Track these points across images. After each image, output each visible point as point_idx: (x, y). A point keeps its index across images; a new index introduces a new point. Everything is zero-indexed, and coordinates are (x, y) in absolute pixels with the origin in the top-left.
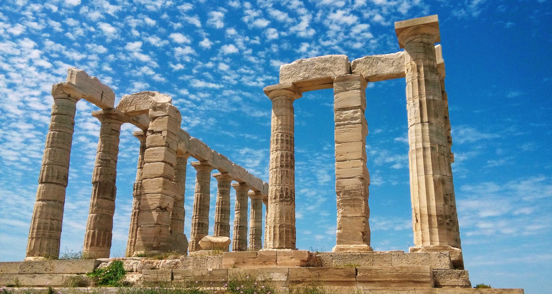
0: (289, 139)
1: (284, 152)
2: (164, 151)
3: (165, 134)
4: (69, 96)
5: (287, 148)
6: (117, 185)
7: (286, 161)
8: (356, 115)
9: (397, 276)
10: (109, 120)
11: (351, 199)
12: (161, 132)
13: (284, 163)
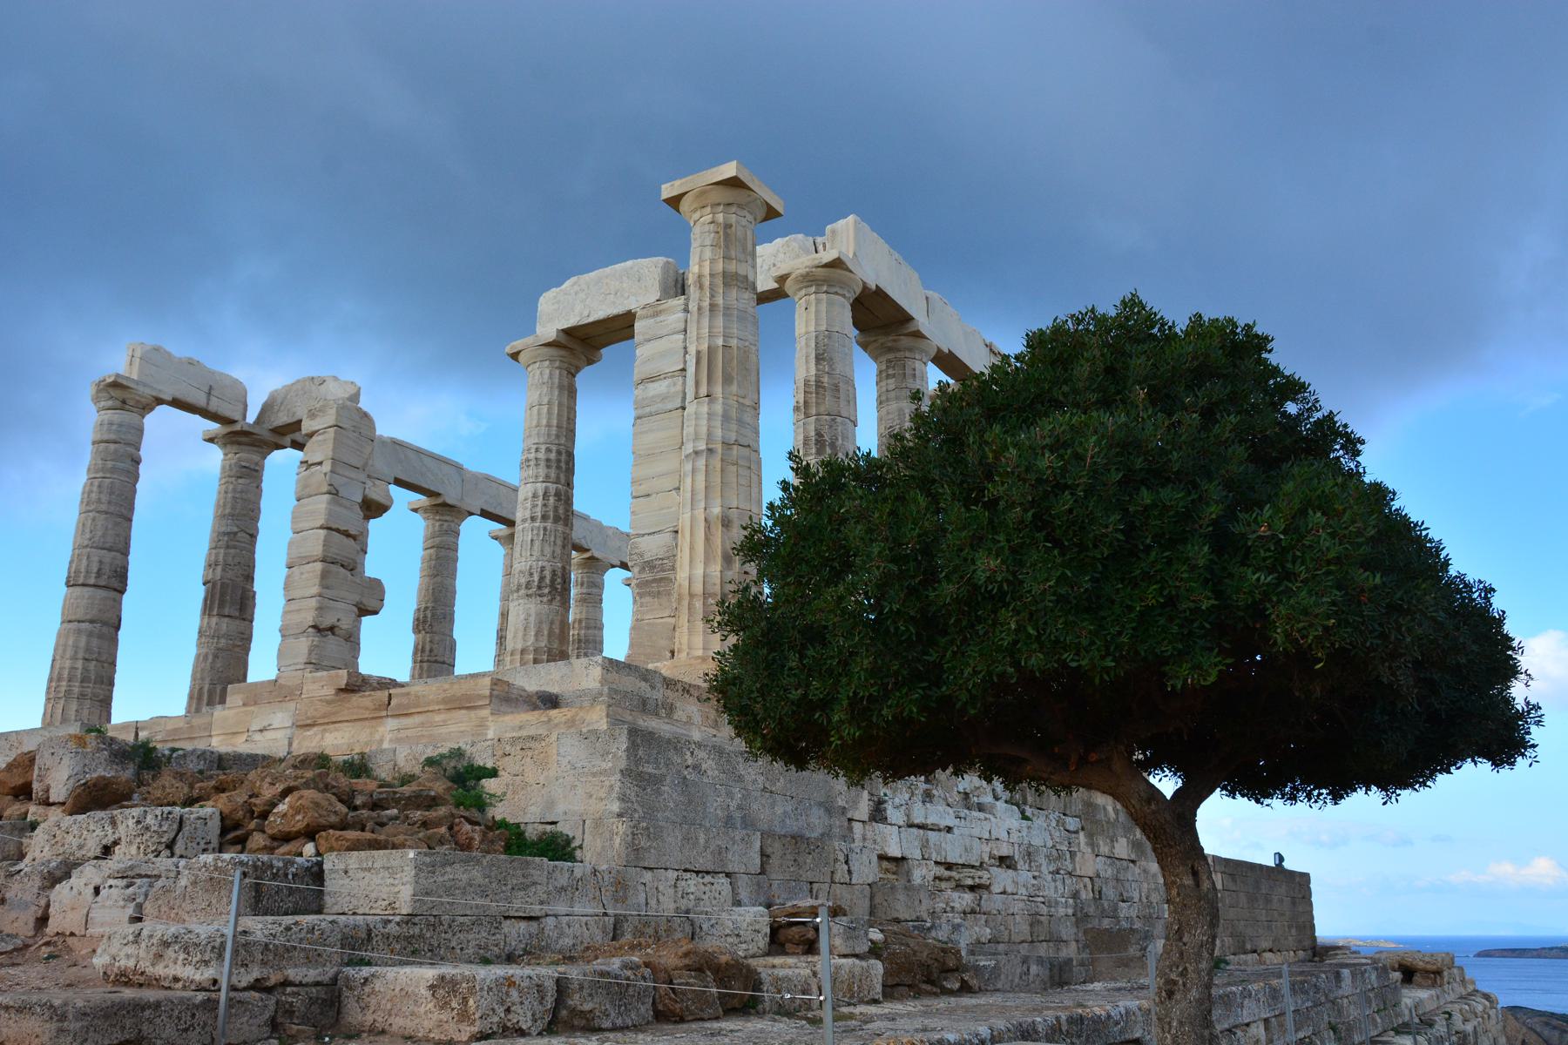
0: (553, 456)
1: (540, 487)
2: (324, 506)
3: (327, 467)
4: (124, 402)
5: (547, 476)
6: (257, 587)
7: (545, 505)
8: (673, 390)
9: (444, 701)
10: (235, 448)
11: (654, 581)
12: (320, 463)
13: (539, 512)
